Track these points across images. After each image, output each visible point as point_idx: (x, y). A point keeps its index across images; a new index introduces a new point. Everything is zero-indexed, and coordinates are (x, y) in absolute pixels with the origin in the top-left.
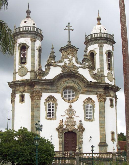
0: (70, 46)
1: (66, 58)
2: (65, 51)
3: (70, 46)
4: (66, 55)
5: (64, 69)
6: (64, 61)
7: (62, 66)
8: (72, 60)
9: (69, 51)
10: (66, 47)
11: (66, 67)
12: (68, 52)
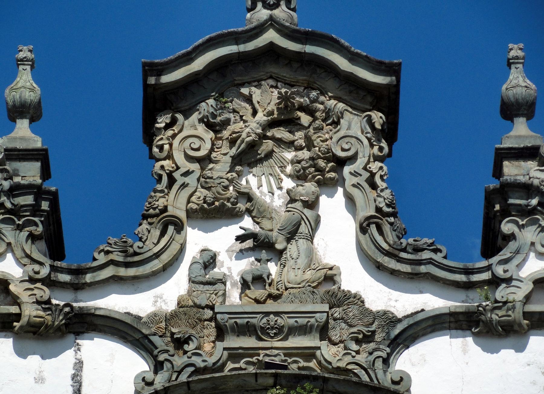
0: (271, 36)
1: (214, 213)
2: (195, 117)
3: (272, 46)
4: (220, 169)
5: (179, 361)
6: (192, 252)
7: (171, 318)
8: (302, 225)
9: (261, 117)
10: (219, 67)
11: (221, 333)
12: (249, 127)
